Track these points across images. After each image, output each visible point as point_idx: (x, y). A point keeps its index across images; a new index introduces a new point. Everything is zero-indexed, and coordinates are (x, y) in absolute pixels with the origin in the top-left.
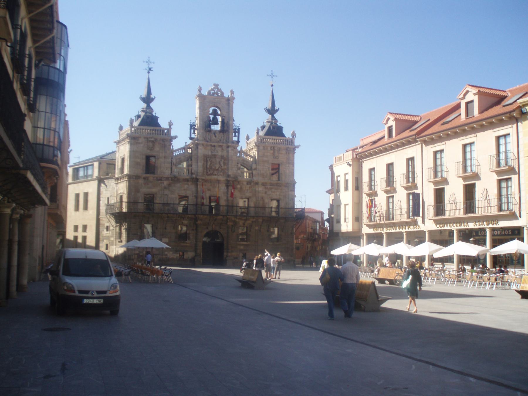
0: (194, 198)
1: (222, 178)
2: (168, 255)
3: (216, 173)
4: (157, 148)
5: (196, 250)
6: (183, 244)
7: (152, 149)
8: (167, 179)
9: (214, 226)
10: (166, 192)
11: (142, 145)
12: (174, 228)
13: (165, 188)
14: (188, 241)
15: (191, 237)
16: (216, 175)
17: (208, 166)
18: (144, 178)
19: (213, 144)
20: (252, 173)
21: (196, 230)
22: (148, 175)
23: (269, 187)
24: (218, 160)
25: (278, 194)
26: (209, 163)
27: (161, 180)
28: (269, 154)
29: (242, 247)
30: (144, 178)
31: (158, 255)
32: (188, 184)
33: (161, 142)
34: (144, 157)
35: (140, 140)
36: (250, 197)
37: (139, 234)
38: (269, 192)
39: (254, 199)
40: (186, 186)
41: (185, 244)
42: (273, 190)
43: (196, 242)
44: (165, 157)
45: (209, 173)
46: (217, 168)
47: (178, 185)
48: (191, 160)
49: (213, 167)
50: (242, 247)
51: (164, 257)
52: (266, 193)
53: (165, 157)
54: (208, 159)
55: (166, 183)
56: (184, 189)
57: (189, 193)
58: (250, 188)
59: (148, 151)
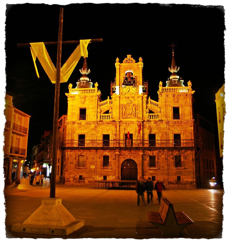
0: (113, 135)
1: (135, 120)
2: (95, 178)
3: (129, 116)
4: (87, 102)
5: (115, 175)
6: (106, 170)
7: (84, 103)
8: (94, 122)
9: (129, 157)
10: (93, 132)
11: (77, 101)
12: (100, 158)
13: (93, 129)
14: (110, 168)
15: (112, 164)
16: (129, 118)
17: (124, 113)
18: (78, 123)
19: (127, 96)
20: (158, 115)
21: (116, 159)
22: (81, 121)
23: (171, 124)
24: (131, 107)
25: (179, 129)
26: (124, 110)
27: (90, 124)
28: (170, 100)
29: (152, 172)
30: (78, 123)
31: (88, 178)
32: (109, 126)
33: (90, 98)
34: (79, 109)
35: (76, 98)
36: (156, 133)
37: (74, 162)
38: (172, 129)
39: (160, 135)
40: (108, 128)
41: (108, 170)
42: (175, 127)
43: (115, 167)
44: (92, 108)
45: (124, 117)
46: (130, 113)
47: (102, 127)
48: (112, 109)
49: (127, 113)
50: (152, 172)
51: (92, 179)
52: (169, 129)
53: (92, 108)
54: (123, 107)
55: (93, 126)
56: (107, 130)
57: (110, 133)
58: (156, 126)
59: (81, 105)
